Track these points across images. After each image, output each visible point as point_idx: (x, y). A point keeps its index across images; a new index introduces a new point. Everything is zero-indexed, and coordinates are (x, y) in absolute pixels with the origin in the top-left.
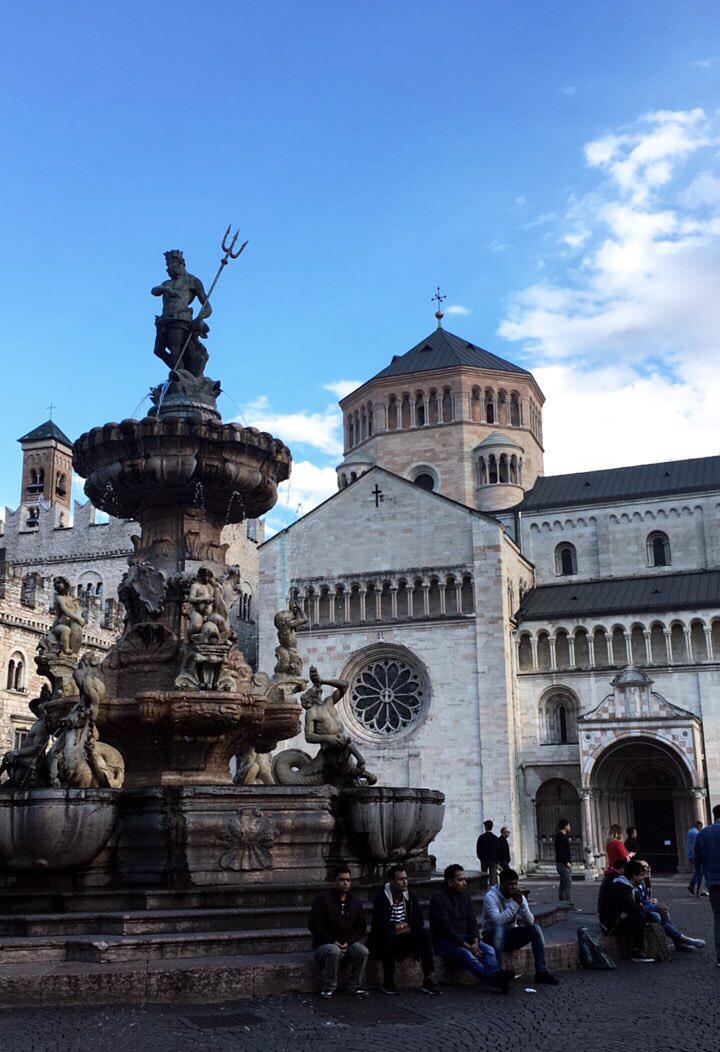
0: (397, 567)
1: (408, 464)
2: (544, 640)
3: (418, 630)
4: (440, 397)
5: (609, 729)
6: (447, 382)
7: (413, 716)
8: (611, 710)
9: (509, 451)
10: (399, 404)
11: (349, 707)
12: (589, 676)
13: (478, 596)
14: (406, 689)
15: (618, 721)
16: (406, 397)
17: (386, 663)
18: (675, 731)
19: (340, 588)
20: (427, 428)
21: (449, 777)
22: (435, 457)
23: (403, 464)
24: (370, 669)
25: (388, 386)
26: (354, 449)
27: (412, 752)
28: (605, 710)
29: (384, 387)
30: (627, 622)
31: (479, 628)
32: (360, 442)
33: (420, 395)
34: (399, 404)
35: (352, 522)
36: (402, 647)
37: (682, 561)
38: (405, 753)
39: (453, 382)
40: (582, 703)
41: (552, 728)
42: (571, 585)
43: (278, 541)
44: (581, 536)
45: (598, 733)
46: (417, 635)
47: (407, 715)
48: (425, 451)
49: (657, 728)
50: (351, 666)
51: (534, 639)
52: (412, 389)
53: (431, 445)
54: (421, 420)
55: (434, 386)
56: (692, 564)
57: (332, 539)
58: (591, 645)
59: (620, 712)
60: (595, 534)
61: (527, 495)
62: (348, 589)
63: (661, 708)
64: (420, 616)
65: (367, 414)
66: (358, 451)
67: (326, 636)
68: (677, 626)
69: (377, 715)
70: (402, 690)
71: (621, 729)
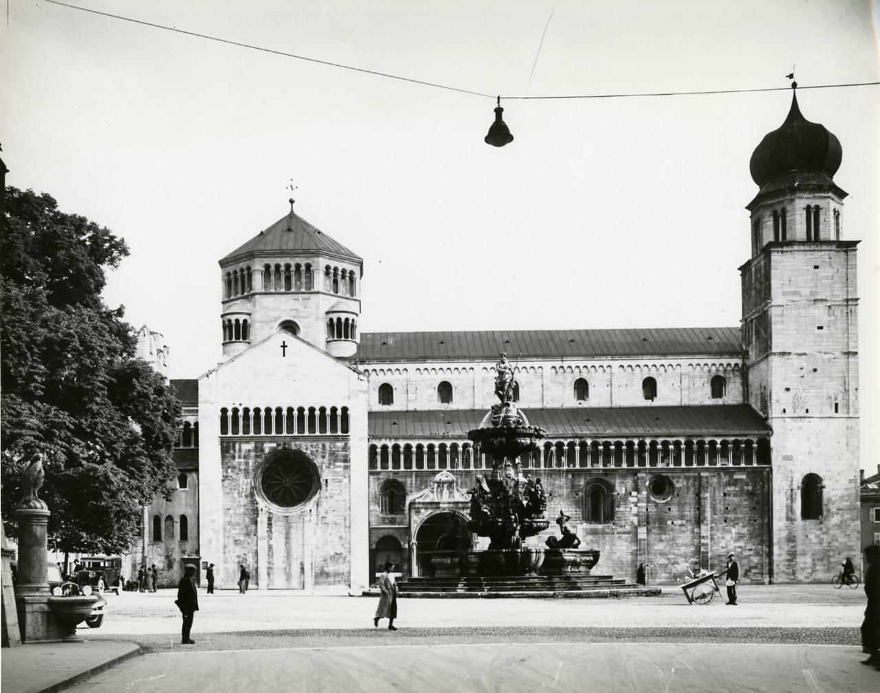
1: (279, 318)
6: (308, 261)
32: (239, 296)
39: (313, 262)
54: (288, 287)
55: (299, 262)
61: (359, 347)
66: (238, 302)
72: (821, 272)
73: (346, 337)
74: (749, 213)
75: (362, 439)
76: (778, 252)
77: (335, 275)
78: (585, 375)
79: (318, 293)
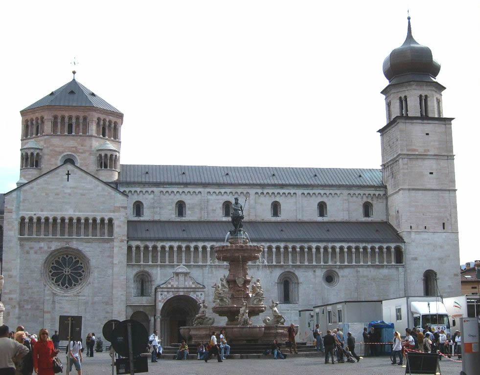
1: (63, 152)
3: (86, 242)
4: (81, 121)
5: (171, 291)
13: (116, 230)
15: (175, 288)
17: (67, 256)
18: (197, 293)
22: (77, 151)
23: (60, 152)
24: (59, 258)
28: (170, 283)
30: (175, 244)
31: (115, 244)
33: (70, 118)
34: (59, 120)
35: (55, 187)
36: (78, 250)
37: (189, 216)
40: (154, 278)
43: (15, 193)
45: (166, 293)
46: (85, 244)
47: (77, 281)
48: (73, 147)
50: (50, 256)
52: (67, 115)
53: (76, 145)
54: (70, 132)
56: (195, 218)
57: (44, 194)
58: (159, 254)
59: (175, 284)
60: (153, 199)
65: (39, 122)
66: (33, 140)
68: (196, 248)
70: (75, 269)
71: (176, 291)
72: (430, 137)
74: (384, 97)
75: (122, 241)
76: (403, 123)
78: (277, 199)
79: (92, 136)
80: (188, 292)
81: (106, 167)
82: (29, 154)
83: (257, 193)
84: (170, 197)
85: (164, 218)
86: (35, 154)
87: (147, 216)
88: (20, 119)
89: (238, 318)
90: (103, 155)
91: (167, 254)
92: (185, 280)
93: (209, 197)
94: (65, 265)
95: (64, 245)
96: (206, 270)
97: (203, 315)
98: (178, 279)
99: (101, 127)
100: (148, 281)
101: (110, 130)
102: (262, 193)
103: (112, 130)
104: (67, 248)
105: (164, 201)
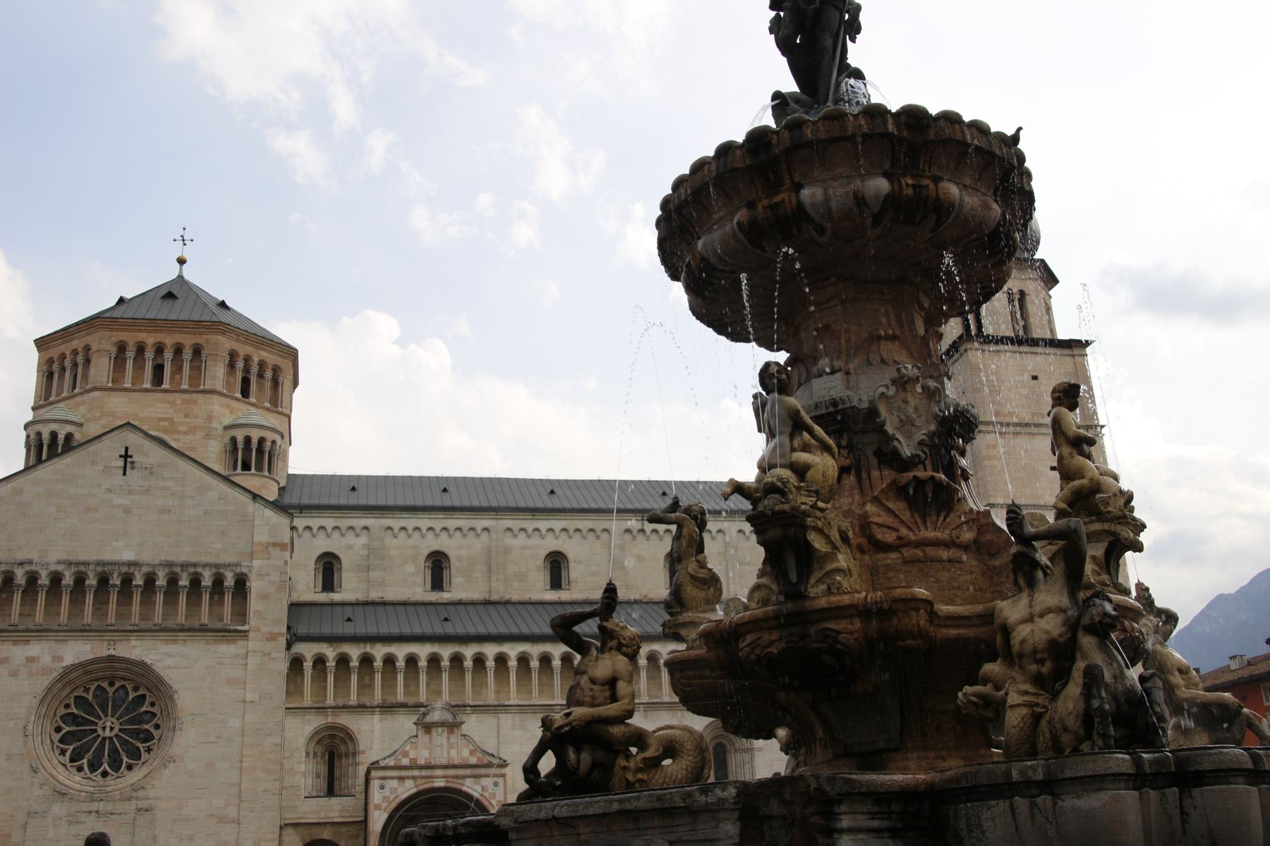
0: (145, 557)
2: (319, 666)
3: (167, 642)
4: (187, 355)
5: (408, 778)
6: (200, 340)
7: (144, 756)
8: (412, 754)
9: (270, 436)
10: (130, 354)
11: (49, 742)
12: (373, 713)
13: (254, 604)
14: (139, 720)
15: (421, 768)
16: (141, 349)
17: (112, 684)
18: (485, 781)
19: (56, 579)
20: (166, 391)
21: (191, 838)
22: (172, 430)
24: (87, 690)
25: (117, 330)
26: (52, 403)
27: (141, 804)
28: (406, 755)
29: (112, 330)
30: (423, 651)
31: (253, 644)
32: (64, 394)
33: (160, 350)
34: (130, 354)
36: (142, 664)
37: (460, 588)
38: (133, 805)
39: (207, 342)
41: (318, 776)
42: (332, 604)
44: (350, 547)
45: (395, 783)
47: (135, 754)
49: (464, 777)
50: (59, 685)
51: (308, 665)
52: (150, 340)
53: (170, 413)
55: (181, 341)
56: (474, 593)
58: (378, 677)
59: (422, 756)
60: (367, 547)
62: (68, 580)
63: (472, 753)
64: (170, 623)
65: (80, 359)
66: (61, 405)
67: (27, 642)
69: (89, 755)
70: (131, 722)
73: (259, 468)
75: (272, 637)
77: (247, 370)
80: (457, 777)
81: (246, 467)
82: (46, 436)
83: (628, 531)
84: (410, 542)
85: (393, 593)
86: (61, 437)
87: (350, 588)
88: (34, 355)
89: (994, 708)
90: (240, 439)
91: (400, 677)
92: (451, 747)
93: (509, 540)
94: (104, 708)
95: (106, 653)
96: (506, 720)
97: (611, 709)
98: (431, 739)
99: (239, 375)
100: (347, 755)
101: (261, 387)
102: (642, 531)
103: (268, 384)
104: (111, 659)
105: (394, 553)
